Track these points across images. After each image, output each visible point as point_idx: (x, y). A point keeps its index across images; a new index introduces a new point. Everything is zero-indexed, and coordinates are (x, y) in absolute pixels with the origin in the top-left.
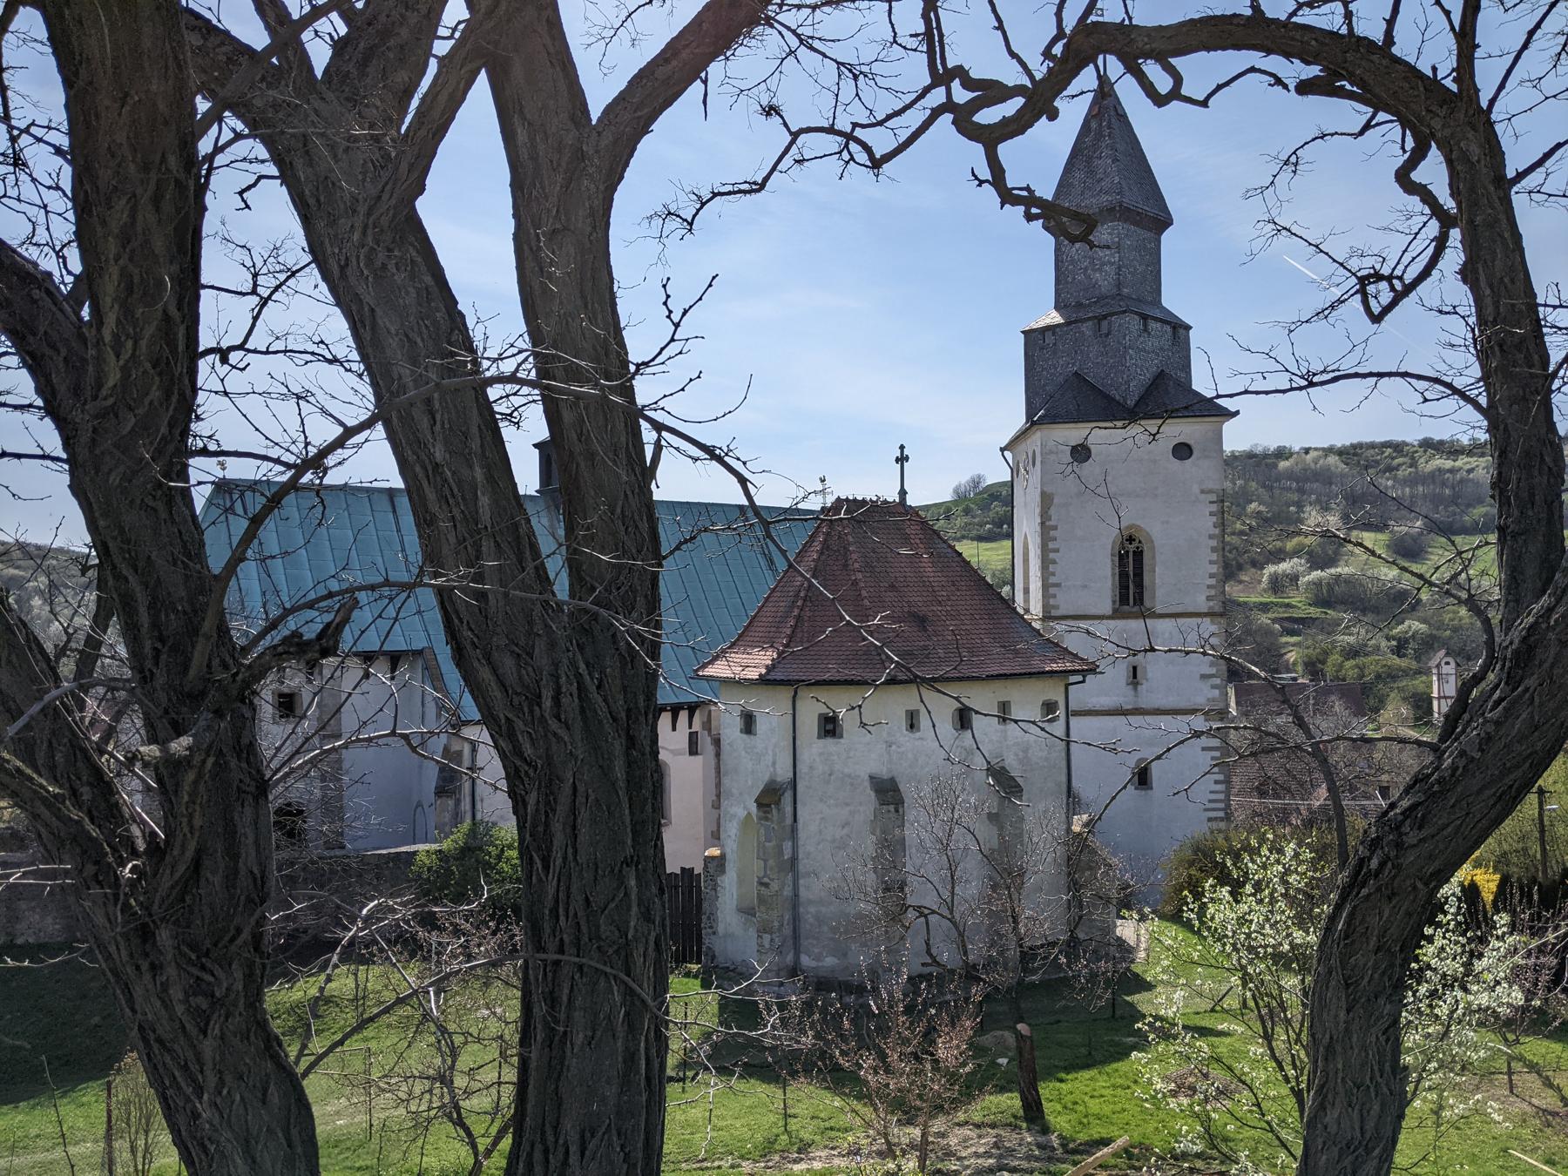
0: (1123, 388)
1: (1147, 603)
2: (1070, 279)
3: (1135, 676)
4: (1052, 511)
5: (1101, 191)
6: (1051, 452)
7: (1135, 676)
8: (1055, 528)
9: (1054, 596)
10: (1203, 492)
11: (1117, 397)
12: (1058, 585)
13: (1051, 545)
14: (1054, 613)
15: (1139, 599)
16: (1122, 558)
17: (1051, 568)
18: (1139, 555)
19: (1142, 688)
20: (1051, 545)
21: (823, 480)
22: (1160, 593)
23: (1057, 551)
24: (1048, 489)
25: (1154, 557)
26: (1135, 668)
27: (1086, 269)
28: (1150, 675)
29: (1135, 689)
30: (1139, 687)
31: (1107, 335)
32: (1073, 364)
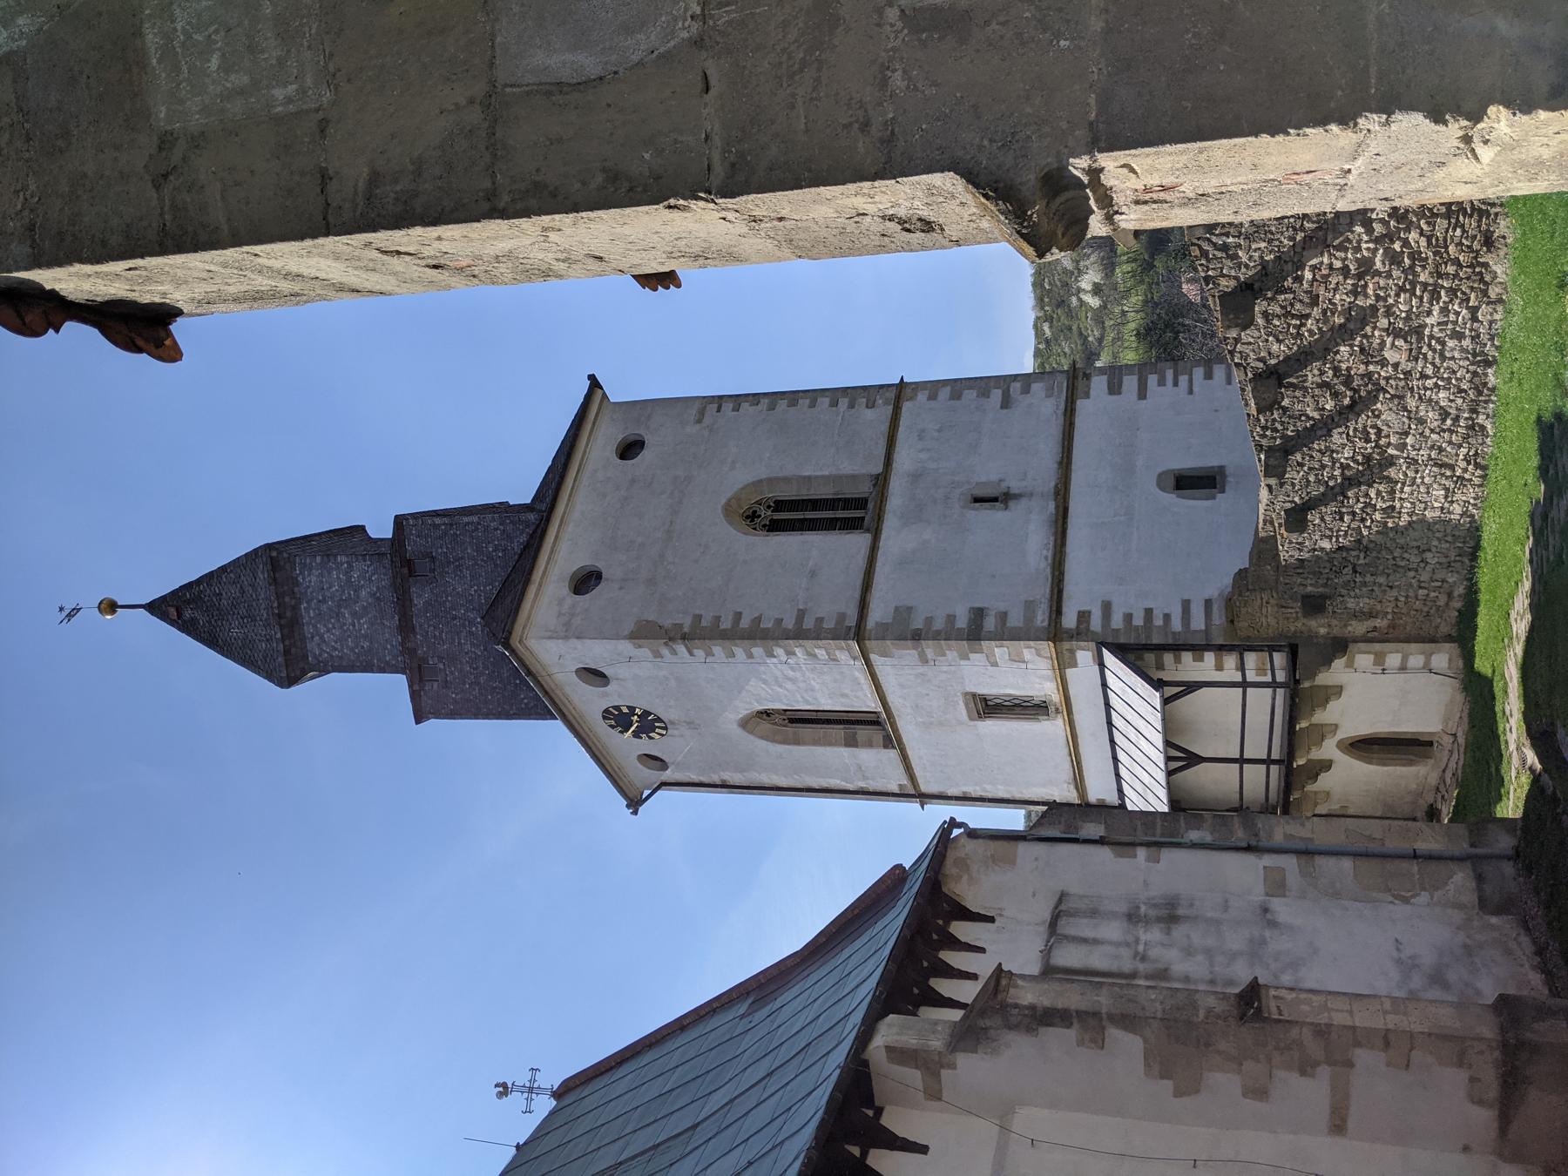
0: (509, 528)
1: (864, 489)
2: (366, 645)
3: (995, 500)
4: (667, 622)
5: (252, 586)
6: (567, 624)
7: (995, 500)
8: (698, 618)
9: (820, 620)
10: (699, 421)
11: (524, 538)
12: (801, 615)
13: (726, 624)
14: (852, 621)
15: (861, 503)
16: (775, 527)
17: (767, 624)
18: (780, 505)
19: (1015, 486)
20: (726, 624)
21: (504, 1090)
22: (847, 467)
23: (738, 616)
24: (629, 626)
25: (787, 480)
26: (977, 500)
27: (354, 614)
28: (994, 477)
29: (1017, 497)
30: (1014, 491)
31: (433, 559)
32: (472, 623)
